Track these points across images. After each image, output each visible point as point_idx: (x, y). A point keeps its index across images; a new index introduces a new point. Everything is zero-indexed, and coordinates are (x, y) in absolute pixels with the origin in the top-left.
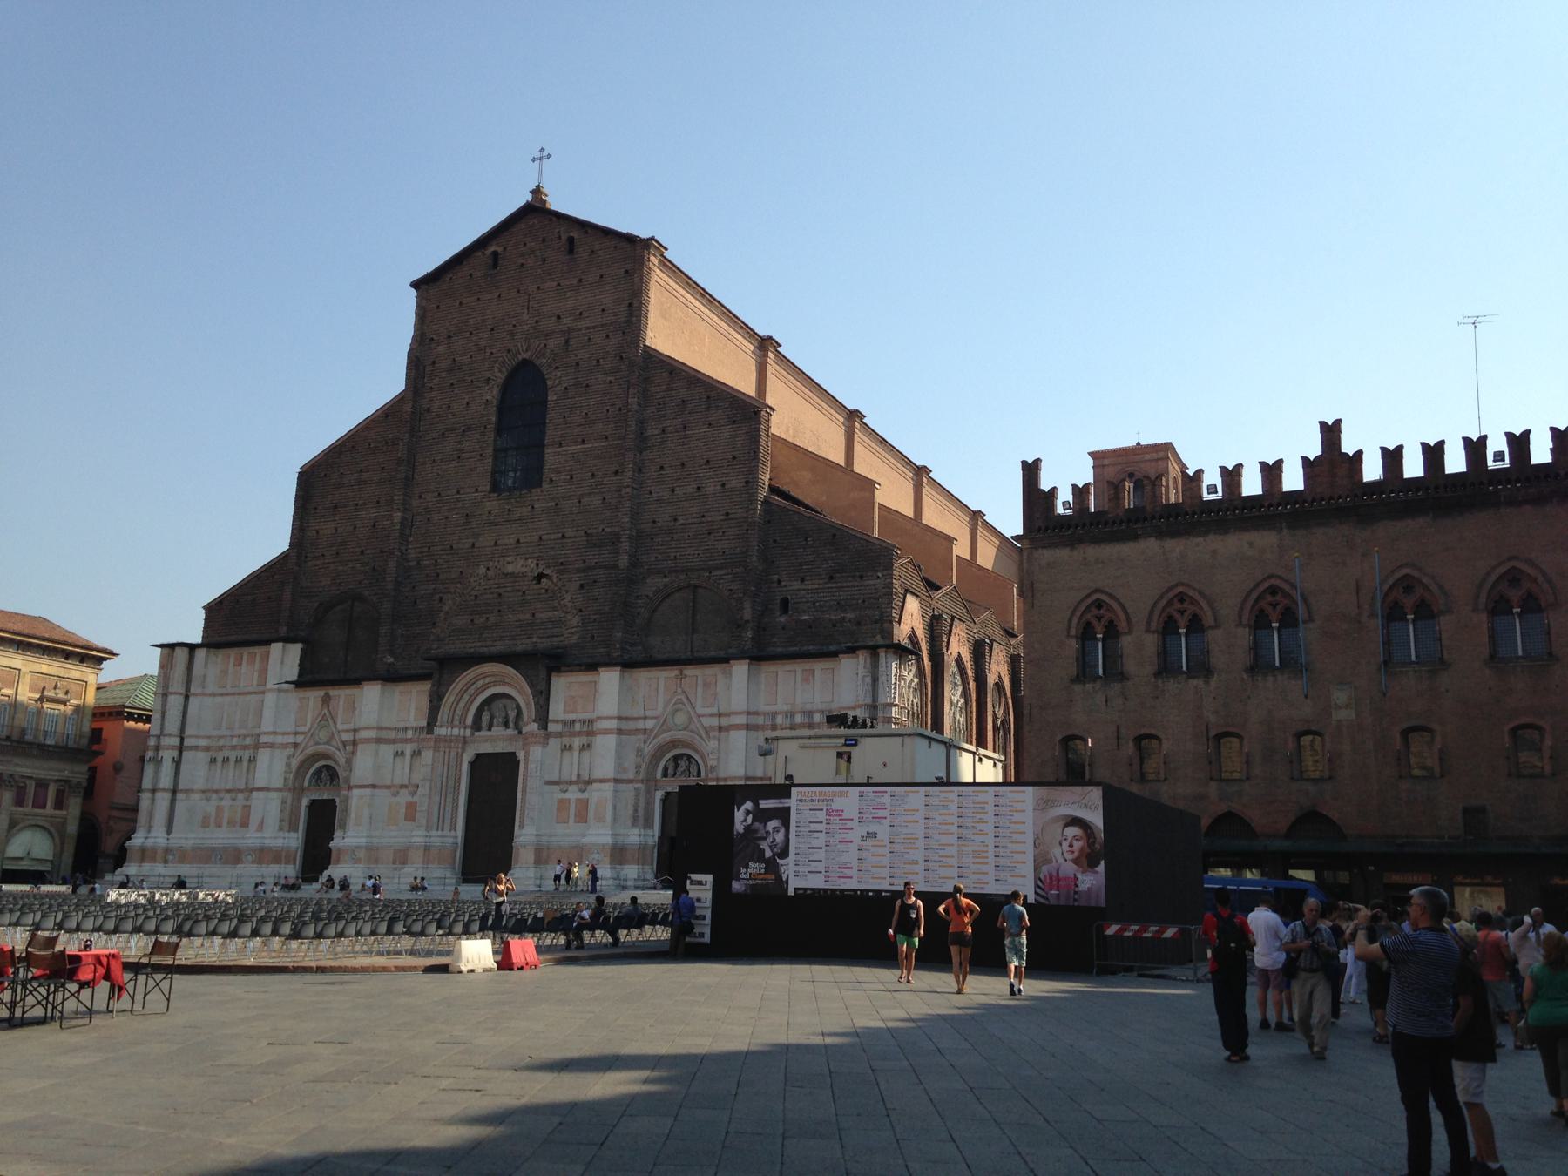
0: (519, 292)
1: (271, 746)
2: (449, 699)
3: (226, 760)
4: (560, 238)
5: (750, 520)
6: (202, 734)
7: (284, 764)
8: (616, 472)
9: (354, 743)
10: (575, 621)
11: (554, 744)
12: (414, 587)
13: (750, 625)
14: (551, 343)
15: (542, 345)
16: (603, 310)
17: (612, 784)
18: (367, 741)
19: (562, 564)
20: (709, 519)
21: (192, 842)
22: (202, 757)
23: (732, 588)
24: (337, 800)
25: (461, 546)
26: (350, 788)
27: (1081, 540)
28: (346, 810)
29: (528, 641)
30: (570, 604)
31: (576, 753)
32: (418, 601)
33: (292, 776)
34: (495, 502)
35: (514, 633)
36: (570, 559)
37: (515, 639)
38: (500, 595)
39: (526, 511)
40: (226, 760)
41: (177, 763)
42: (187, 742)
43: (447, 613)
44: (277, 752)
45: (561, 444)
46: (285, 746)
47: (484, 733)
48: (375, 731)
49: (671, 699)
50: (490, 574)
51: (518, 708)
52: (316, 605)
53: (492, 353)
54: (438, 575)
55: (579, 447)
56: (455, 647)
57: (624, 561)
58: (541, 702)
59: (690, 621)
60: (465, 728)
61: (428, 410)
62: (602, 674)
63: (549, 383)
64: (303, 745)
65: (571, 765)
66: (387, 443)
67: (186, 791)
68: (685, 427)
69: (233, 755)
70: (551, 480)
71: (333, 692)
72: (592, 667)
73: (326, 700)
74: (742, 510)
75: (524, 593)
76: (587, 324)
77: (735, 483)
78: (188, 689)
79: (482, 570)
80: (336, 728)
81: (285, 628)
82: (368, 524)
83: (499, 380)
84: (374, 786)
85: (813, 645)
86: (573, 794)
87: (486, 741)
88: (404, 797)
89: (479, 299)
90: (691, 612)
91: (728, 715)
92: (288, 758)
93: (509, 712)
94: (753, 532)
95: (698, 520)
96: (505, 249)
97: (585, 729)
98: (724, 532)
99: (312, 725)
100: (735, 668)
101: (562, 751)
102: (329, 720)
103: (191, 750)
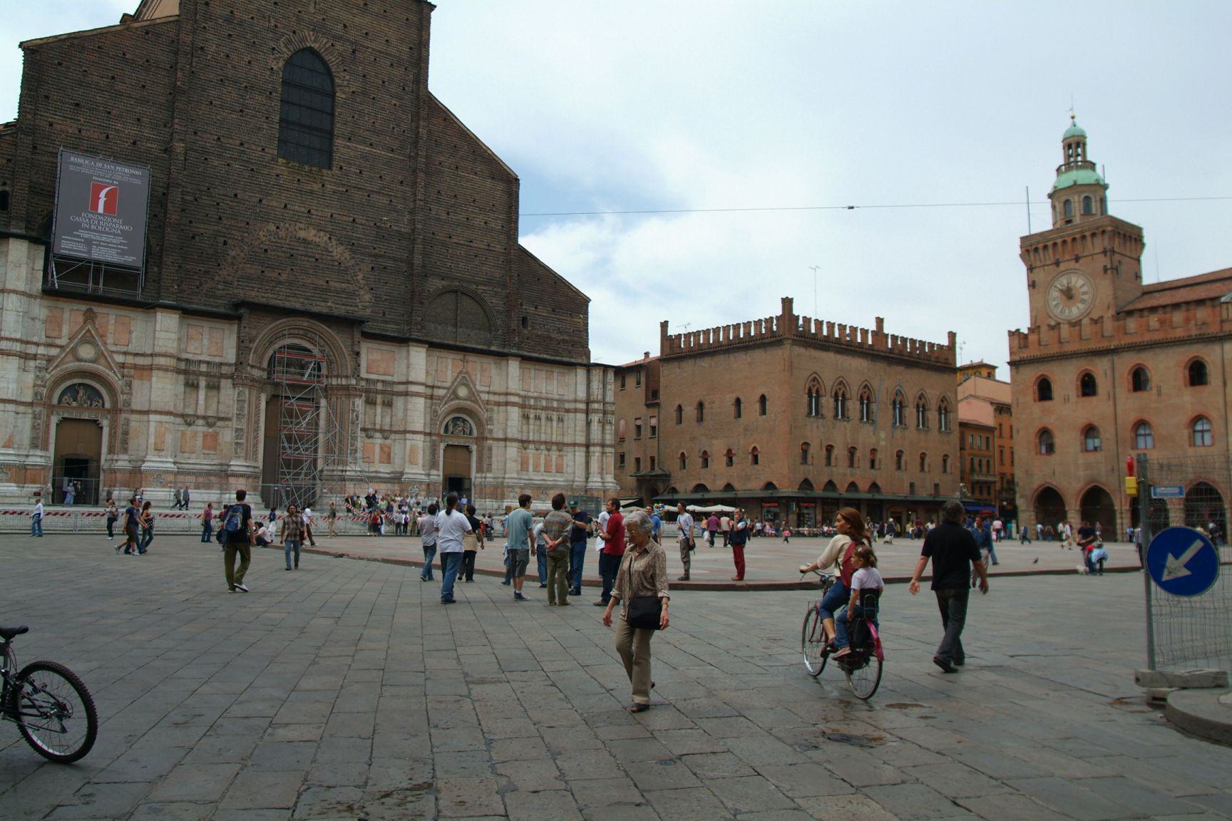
8: (402, 182)
9: (151, 368)
10: (367, 297)
12: (191, 222)
14: (338, 46)
16: (387, 41)
17: (422, 436)
19: (353, 244)
26: (133, 412)
27: (810, 346)
29: (322, 304)
31: (379, 409)
32: (197, 238)
35: (307, 294)
39: (316, 187)
43: (234, 258)
45: (349, 139)
50: (282, 233)
53: (276, 26)
54: (220, 219)
55: (368, 149)
59: (459, 318)
60: (263, 370)
62: (411, 348)
63: (337, 80)
64: (59, 360)
65: (380, 416)
66: (147, 61)
68: (457, 168)
70: (341, 168)
71: (99, 310)
75: (317, 260)
76: (373, 45)
80: (107, 350)
82: (125, 140)
83: (286, 56)
85: (548, 354)
86: (378, 440)
88: (200, 428)
91: (500, 394)
92: (39, 369)
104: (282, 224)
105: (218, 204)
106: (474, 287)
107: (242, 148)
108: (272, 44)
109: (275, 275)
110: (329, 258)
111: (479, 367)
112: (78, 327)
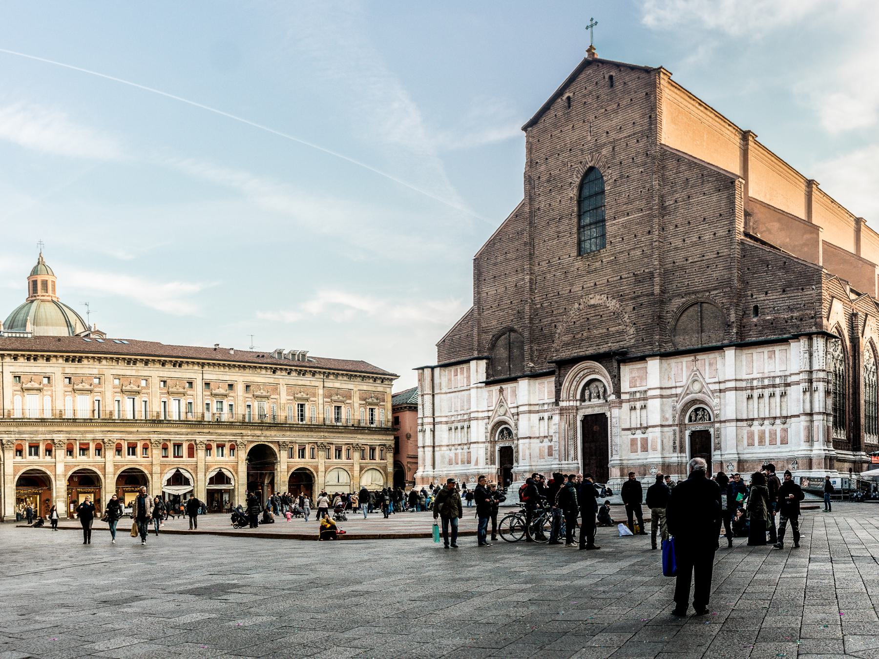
1: (477, 419)
2: (566, 385)
3: (456, 428)
5: (731, 256)
6: (443, 415)
7: (485, 426)
9: (518, 414)
10: (632, 331)
11: (626, 406)
13: (735, 325)
18: (524, 412)
20: (708, 257)
21: (445, 472)
22: (445, 427)
23: (723, 301)
24: (513, 447)
25: (563, 292)
26: (518, 439)
28: (517, 452)
29: (606, 346)
30: (628, 321)
33: (489, 435)
34: (580, 262)
36: (626, 292)
37: (598, 345)
38: (588, 319)
39: (598, 264)
40: (456, 428)
41: (433, 431)
42: (437, 420)
43: (559, 334)
44: (480, 421)
46: (483, 418)
47: (587, 403)
48: (527, 406)
49: (690, 375)
50: (581, 307)
51: (604, 386)
52: (491, 336)
54: (553, 312)
56: (565, 354)
57: (657, 290)
58: (616, 382)
59: (700, 325)
60: (577, 400)
67: (440, 446)
69: (459, 425)
71: (504, 386)
72: (643, 358)
73: (501, 391)
74: (725, 250)
77: (722, 232)
78: (433, 391)
79: (576, 306)
81: (476, 352)
84: (530, 438)
87: (589, 408)
90: (700, 319)
93: (600, 389)
94: (734, 264)
95: (699, 259)
97: (642, 396)
98: (717, 265)
100: (726, 352)
101: (631, 410)
104: (581, 300)
106: (707, 294)
109: (580, 335)
110: (608, 312)
111: (707, 364)
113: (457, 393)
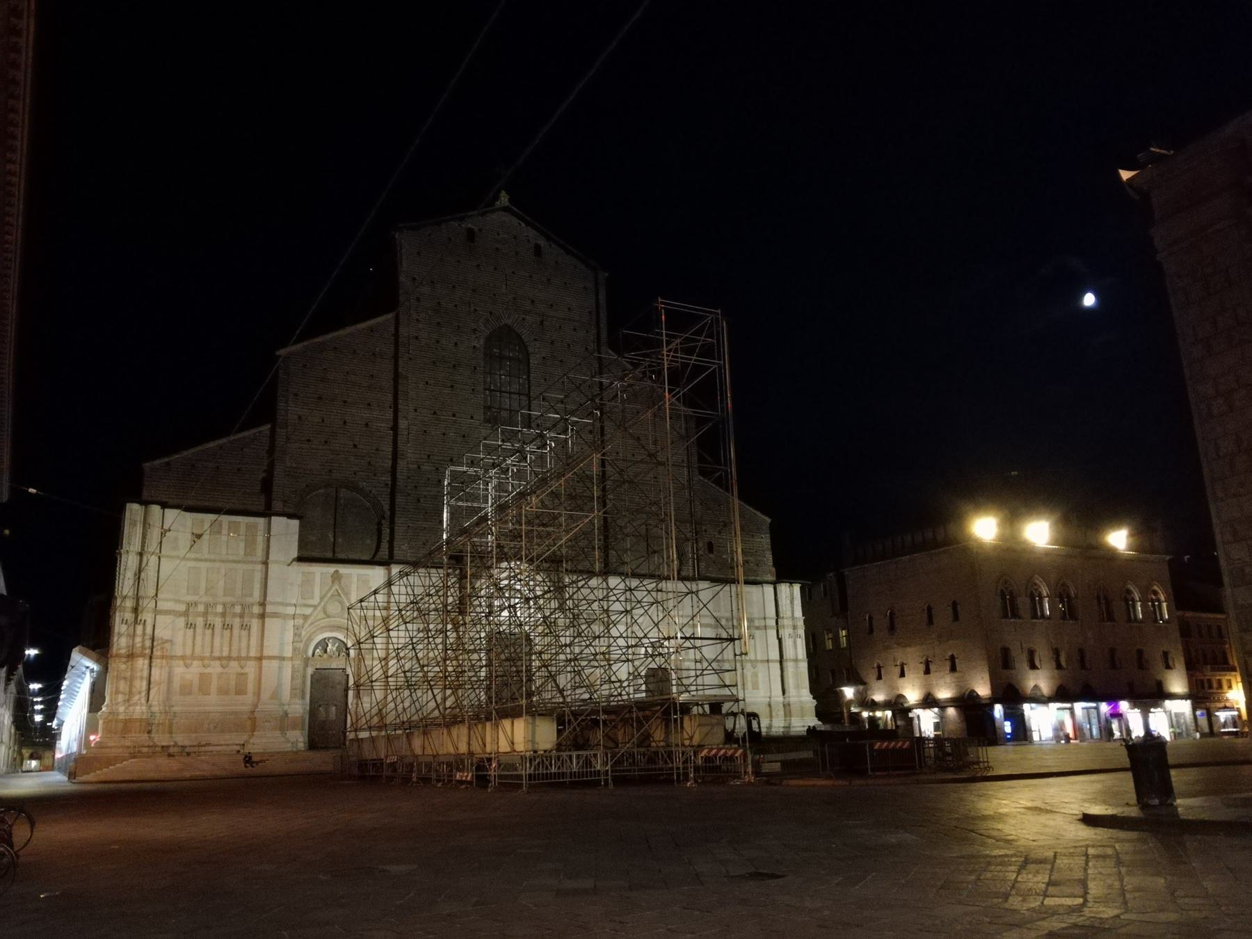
0: (495, 269)
4: (529, 241)
15: (521, 319)
22: (181, 621)
32: (421, 499)
53: (475, 310)
61: (417, 338)
63: (530, 350)
71: (344, 570)
82: (359, 422)
89: (459, 261)
92: (296, 628)
96: (480, 230)
99: (322, 599)
102: (342, 595)
103: (170, 614)
105: (437, 469)
107: (454, 418)
108: (474, 326)
112: (327, 588)
113: (217, 565)
